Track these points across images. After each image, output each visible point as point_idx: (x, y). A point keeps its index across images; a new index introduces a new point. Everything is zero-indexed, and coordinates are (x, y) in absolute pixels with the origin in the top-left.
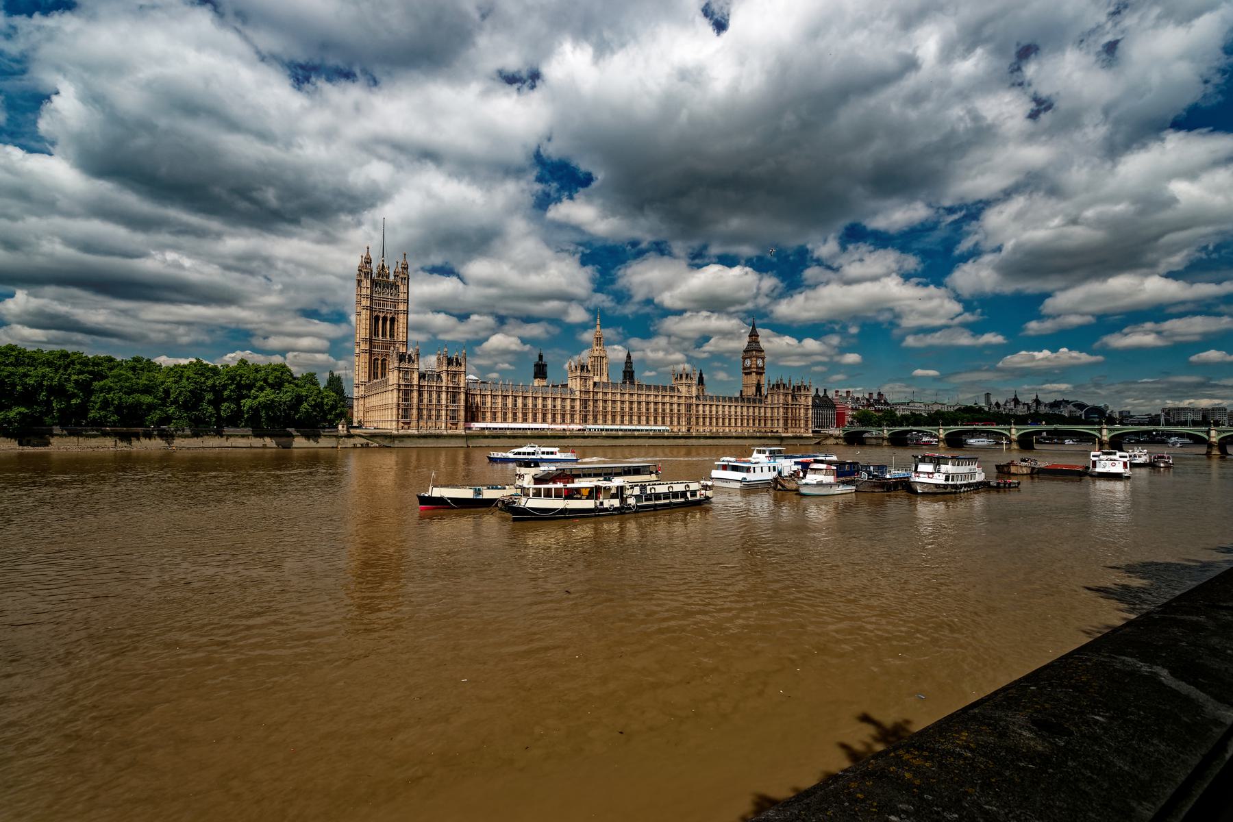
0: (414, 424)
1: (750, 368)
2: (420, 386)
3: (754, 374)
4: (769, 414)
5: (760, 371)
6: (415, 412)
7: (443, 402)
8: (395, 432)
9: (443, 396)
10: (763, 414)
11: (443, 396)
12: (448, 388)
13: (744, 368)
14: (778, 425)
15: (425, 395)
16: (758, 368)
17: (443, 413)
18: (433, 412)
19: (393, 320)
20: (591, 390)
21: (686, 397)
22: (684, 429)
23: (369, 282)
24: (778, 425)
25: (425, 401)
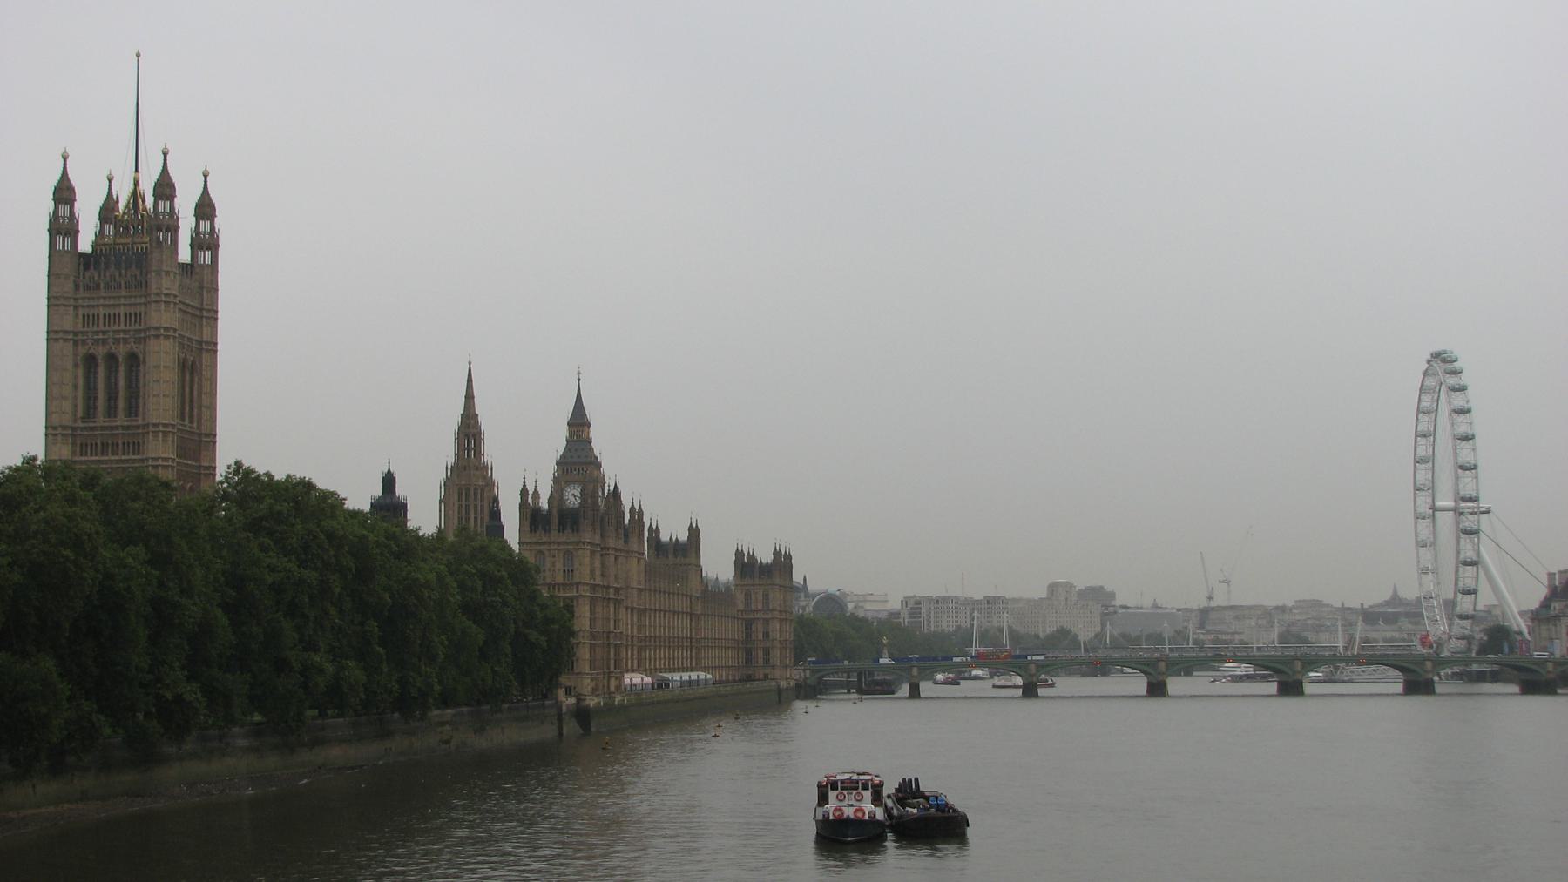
14: (767, 661)
24: (767, 661)
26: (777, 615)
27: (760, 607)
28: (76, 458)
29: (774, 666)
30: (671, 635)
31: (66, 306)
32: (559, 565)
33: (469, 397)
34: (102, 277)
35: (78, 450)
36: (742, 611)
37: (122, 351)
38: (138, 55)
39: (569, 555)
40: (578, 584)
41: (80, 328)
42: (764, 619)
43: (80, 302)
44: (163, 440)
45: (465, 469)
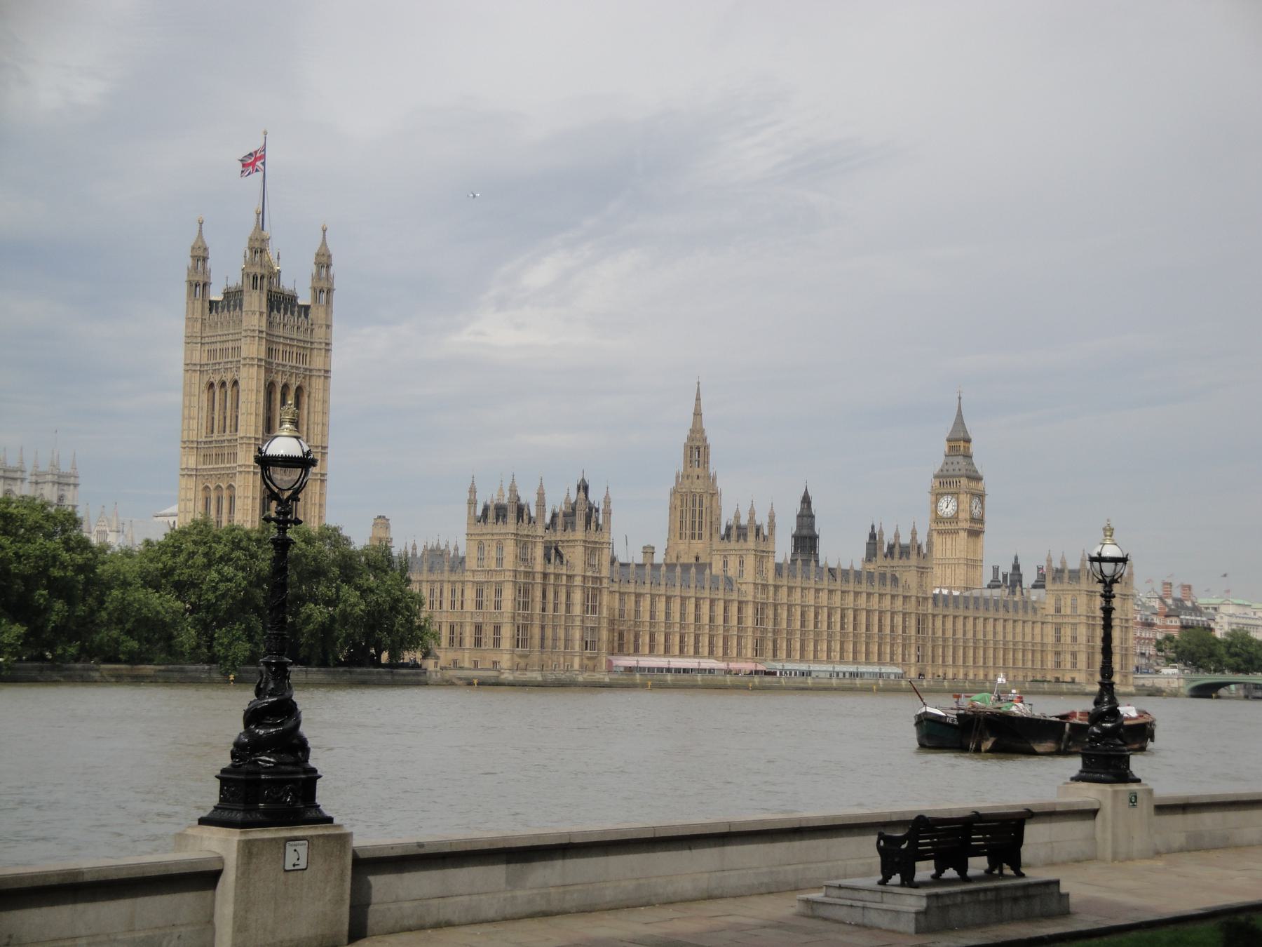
0: (535, 657)
1: (955, 518)
2: (545, 576)
3: (963, 535)
4: (1050, 639)
5: (976, 526)
6: (536, 632)
7: (577, 610)
8: (507, 676)
9: (577, 597)
10: (1038, 639)
11: (577, 597)
12: (584, 577)
13: (938, 519)
14: (1074, 665)
15: (550, 596)
16: (973, 520)
17: (577, 634)
18: (561, 633)
19: (299, 389)
20: (771, 582)
21: (917, 597)
22: (913, 673)
23: (264, 299)
24: (1074, 665)
25: (550, 607)
26: (1084, 619)
27: (1069, 611)
28: (199, 467)
29: (1079, 670)
30: (1019, 638)
31: (196, 343)
32: (493, 554)
33: (698, 414)
34: (219, 319)
35: (202, 460)
36: (1052, 615)
37: (228, 378)
38: (265, 133)
39: (500, 548)
40: (504, 570)
41: (204, 361)
42: (1072, 624)
43: (207, 340)
44: (246, 451)
45: (688, 478)
